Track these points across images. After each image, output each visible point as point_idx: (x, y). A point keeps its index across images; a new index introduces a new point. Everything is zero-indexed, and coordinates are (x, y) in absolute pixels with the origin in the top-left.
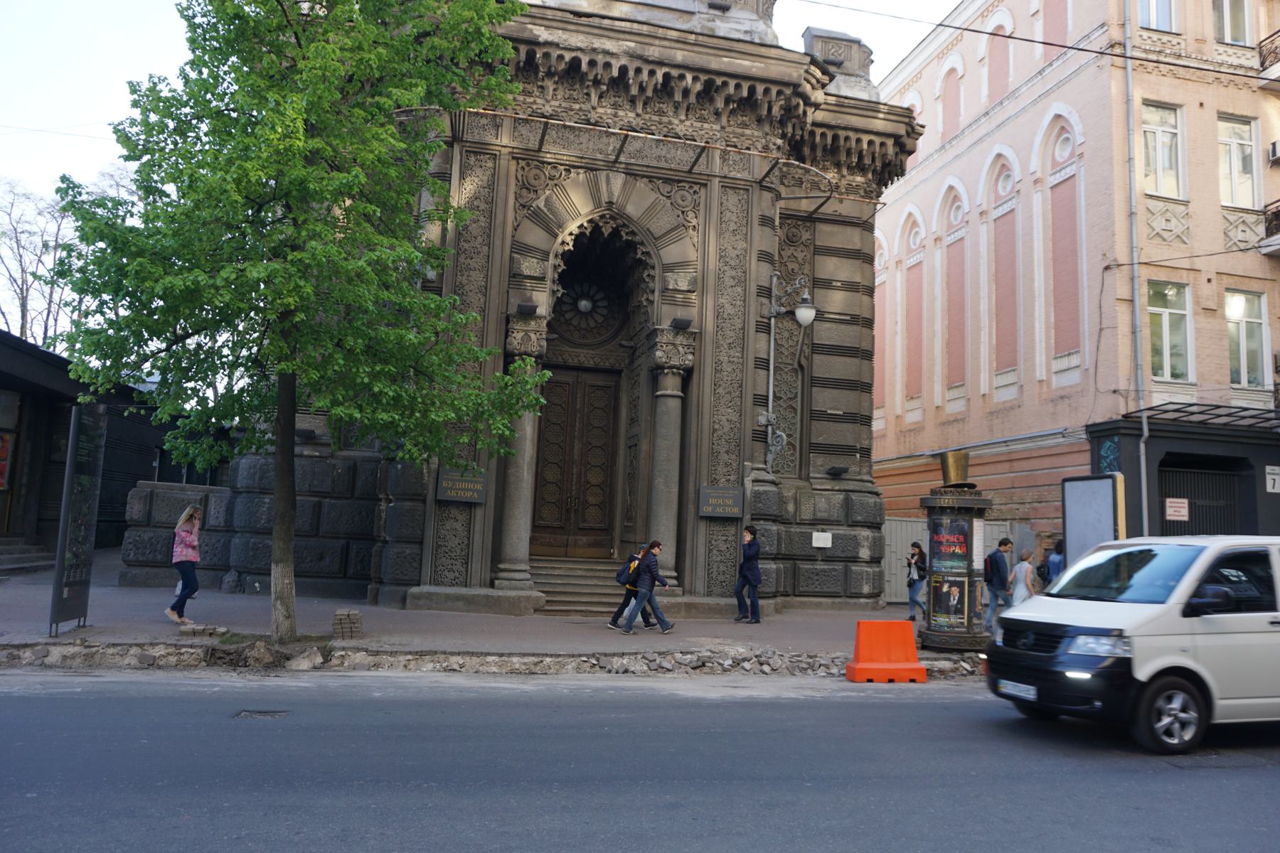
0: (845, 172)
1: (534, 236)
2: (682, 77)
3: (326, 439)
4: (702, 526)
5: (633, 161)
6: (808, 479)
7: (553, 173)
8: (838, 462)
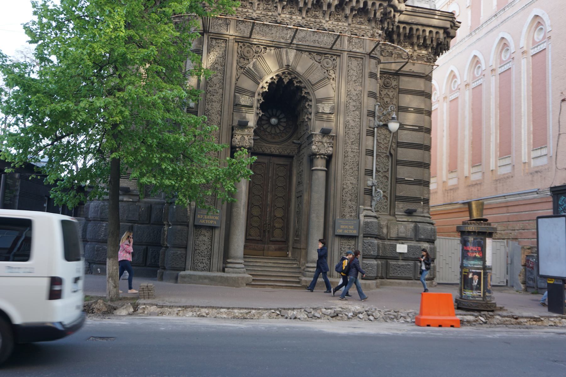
0: (416, 48)
1: (247, 84)
3: (135, 192)
4: (337, 240)
5: (300, 43)
6: (394, 215)
7: (257, 49)
8: (411, 206)
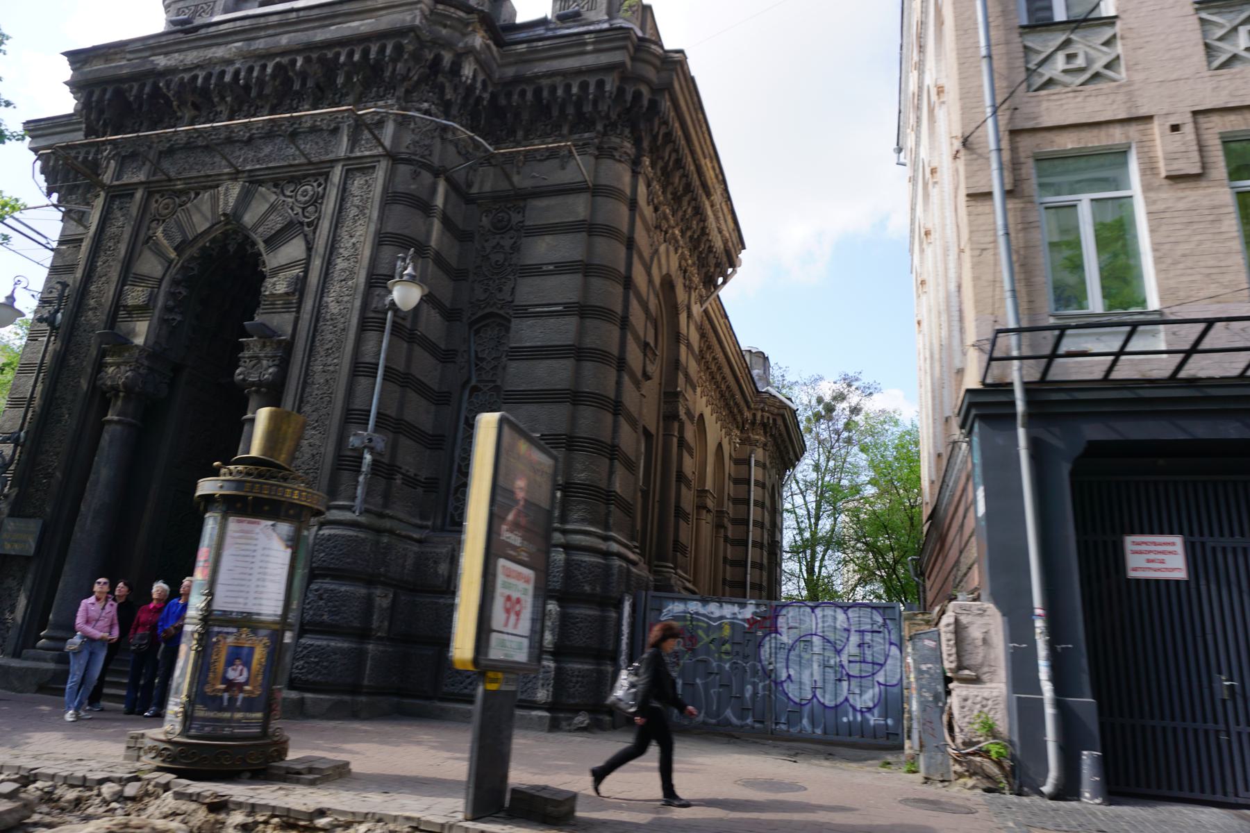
2: (294, 62)
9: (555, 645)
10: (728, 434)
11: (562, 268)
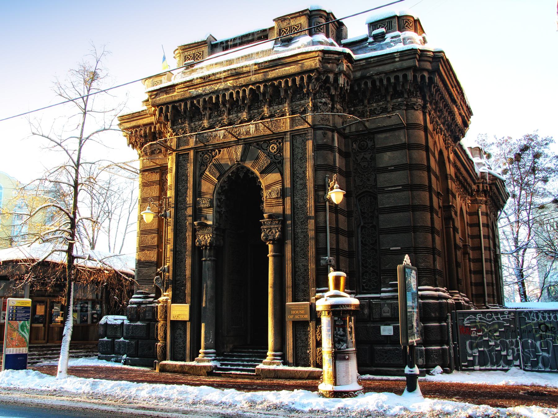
0: (389, 99)
9: (423, 340)
10: (464, 200)
11: (398, 168)
